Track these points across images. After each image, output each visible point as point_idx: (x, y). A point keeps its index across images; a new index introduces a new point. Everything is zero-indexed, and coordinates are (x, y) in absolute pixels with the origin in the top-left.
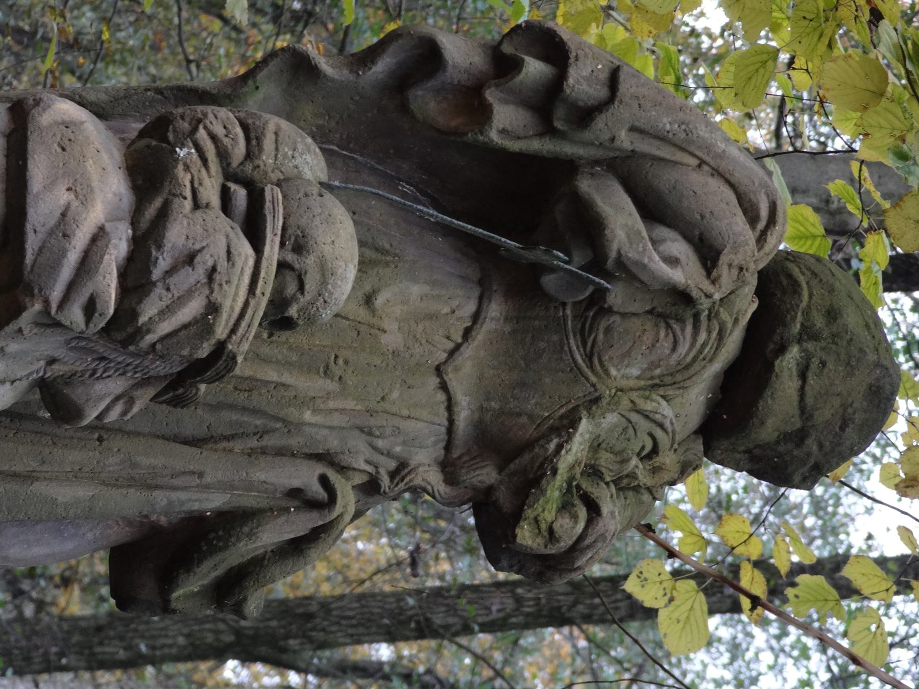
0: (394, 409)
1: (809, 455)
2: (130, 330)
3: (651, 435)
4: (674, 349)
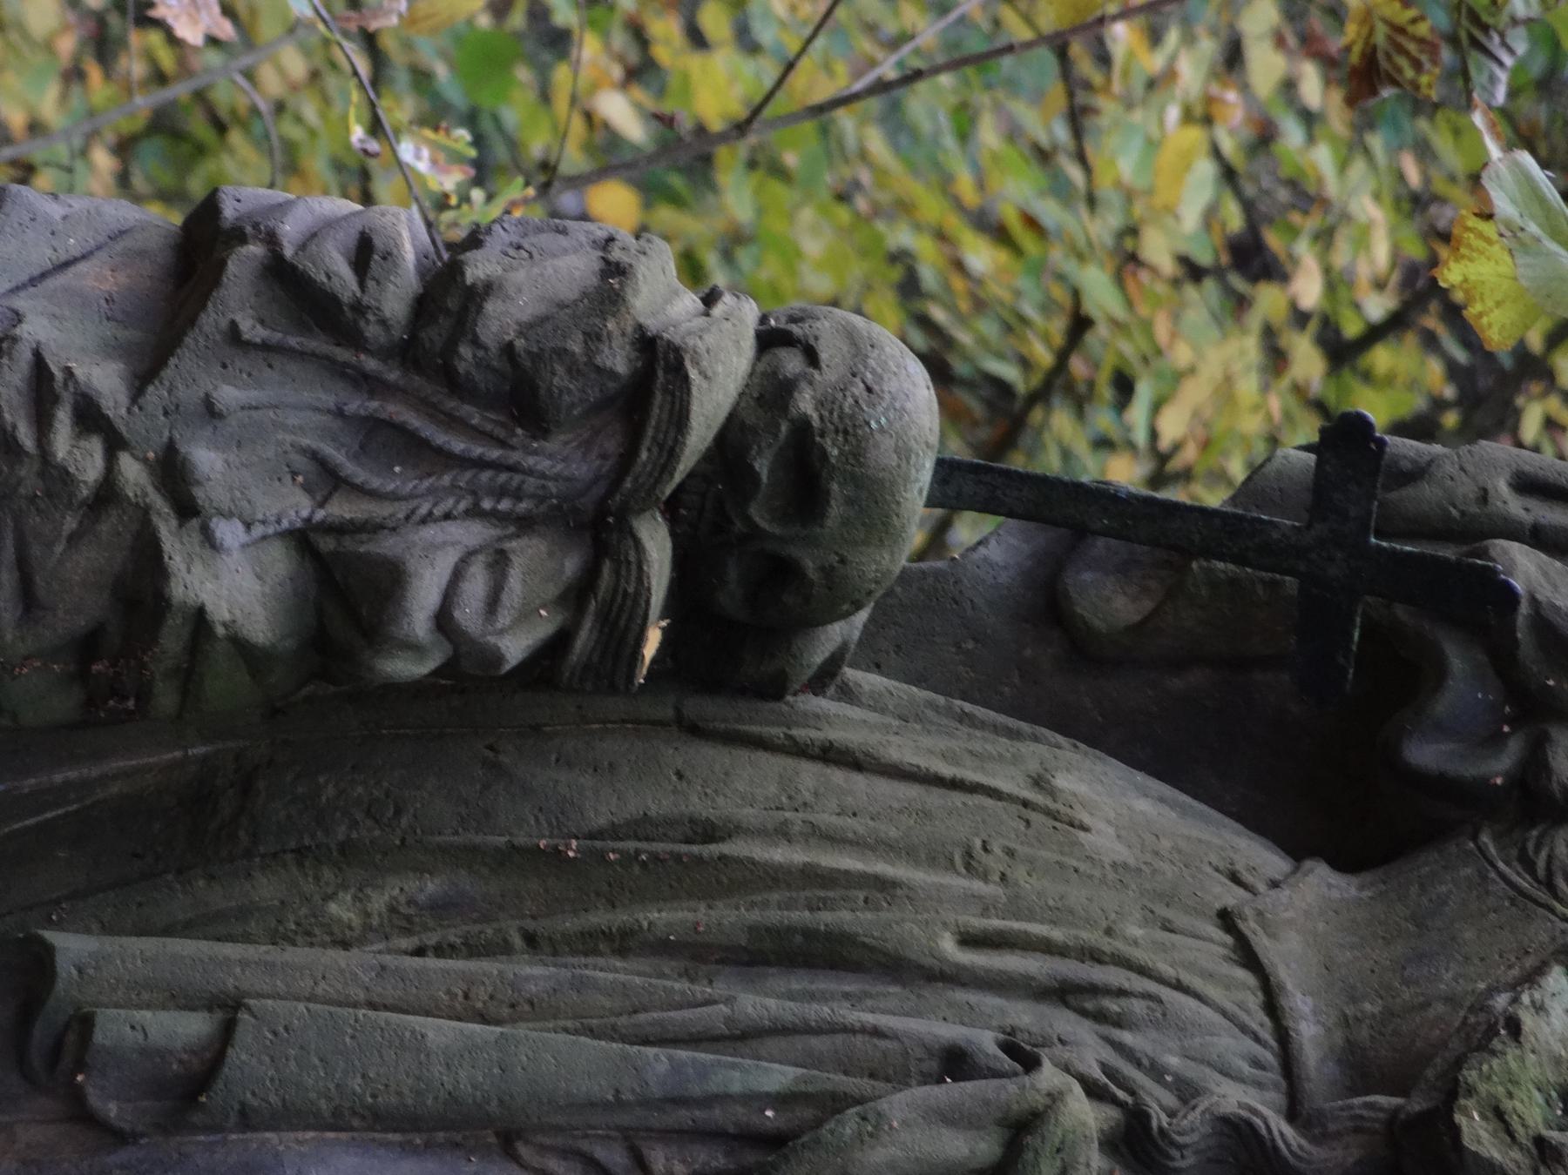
0: (1140, 955)
2: (452, 303)
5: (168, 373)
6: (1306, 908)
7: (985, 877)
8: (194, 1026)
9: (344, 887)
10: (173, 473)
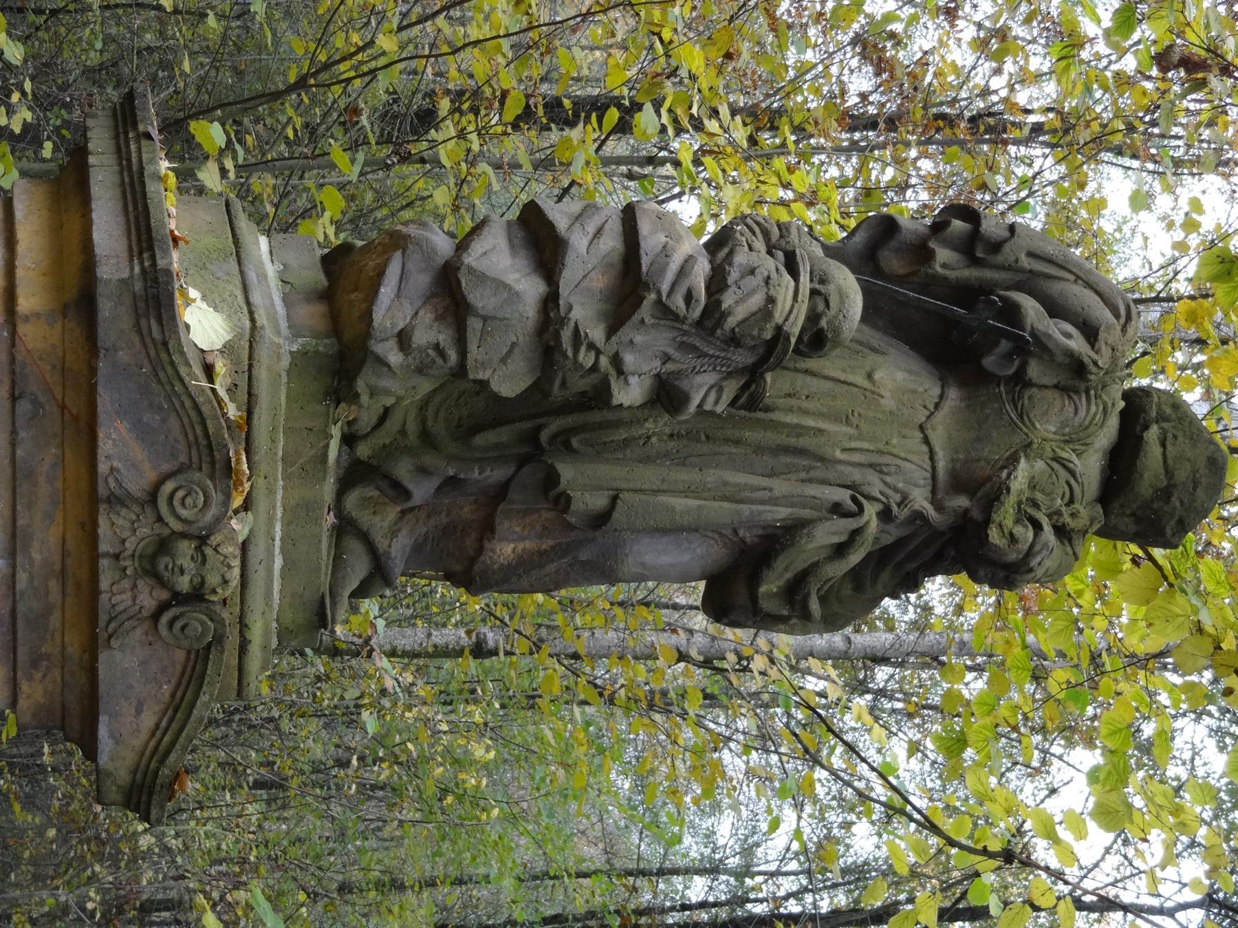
0: (895, 451)
1: (1175, 509)
2: (717, 316)
3: (1068, 483)
4: (1076, 413)
5: (619, 333)
7: (851, 426)
9: (650, 416)
10: (616, 361)
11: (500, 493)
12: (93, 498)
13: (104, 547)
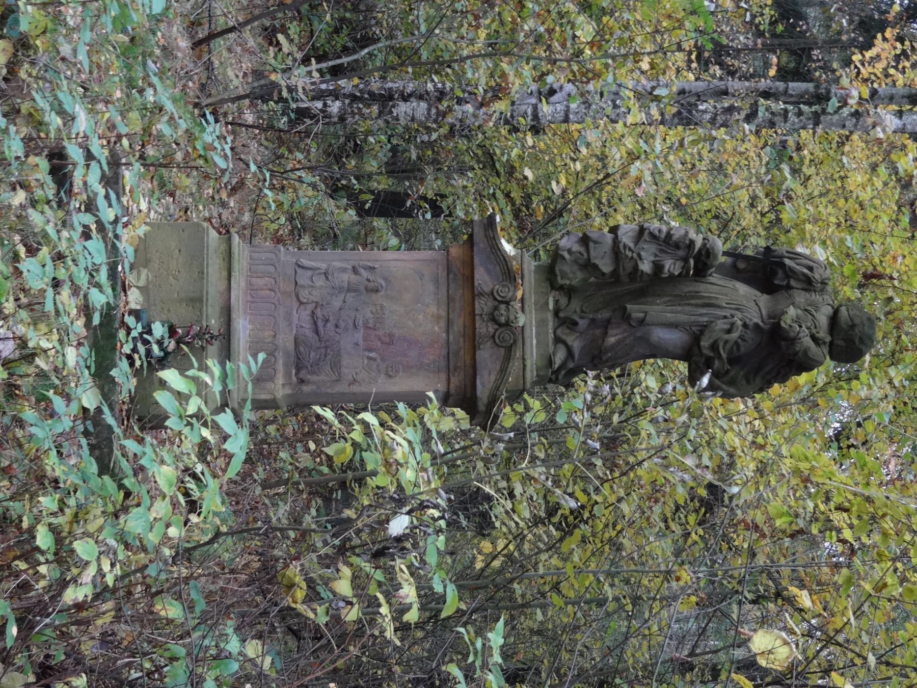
6: (764, 300)
8: (642, 315)
10: (639, 255)
11: (608, 321)
12: (473, 293)
13: (477, 312)
